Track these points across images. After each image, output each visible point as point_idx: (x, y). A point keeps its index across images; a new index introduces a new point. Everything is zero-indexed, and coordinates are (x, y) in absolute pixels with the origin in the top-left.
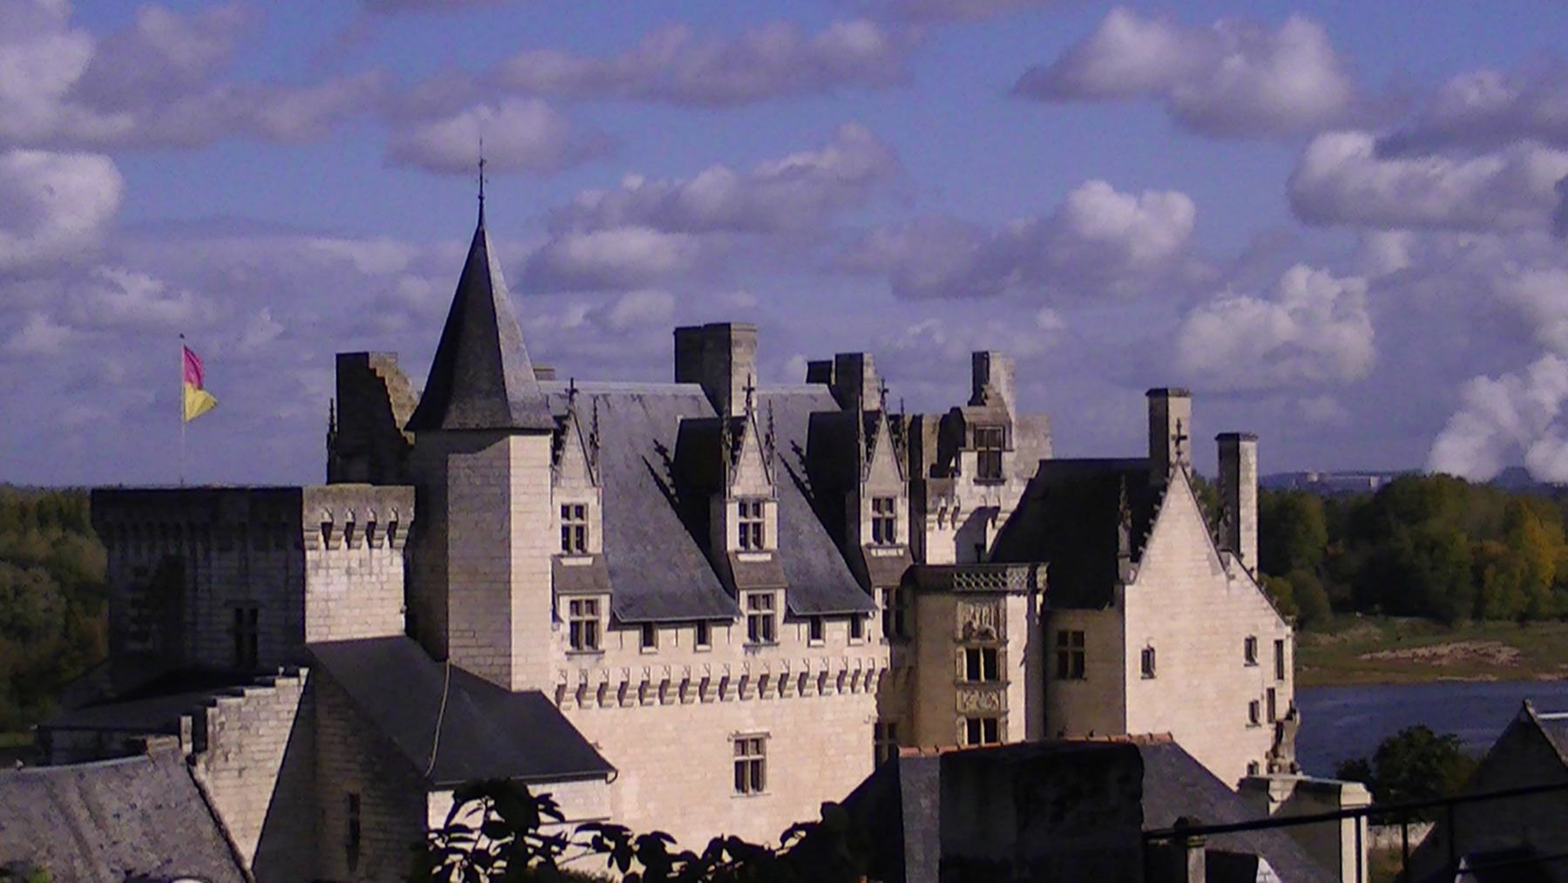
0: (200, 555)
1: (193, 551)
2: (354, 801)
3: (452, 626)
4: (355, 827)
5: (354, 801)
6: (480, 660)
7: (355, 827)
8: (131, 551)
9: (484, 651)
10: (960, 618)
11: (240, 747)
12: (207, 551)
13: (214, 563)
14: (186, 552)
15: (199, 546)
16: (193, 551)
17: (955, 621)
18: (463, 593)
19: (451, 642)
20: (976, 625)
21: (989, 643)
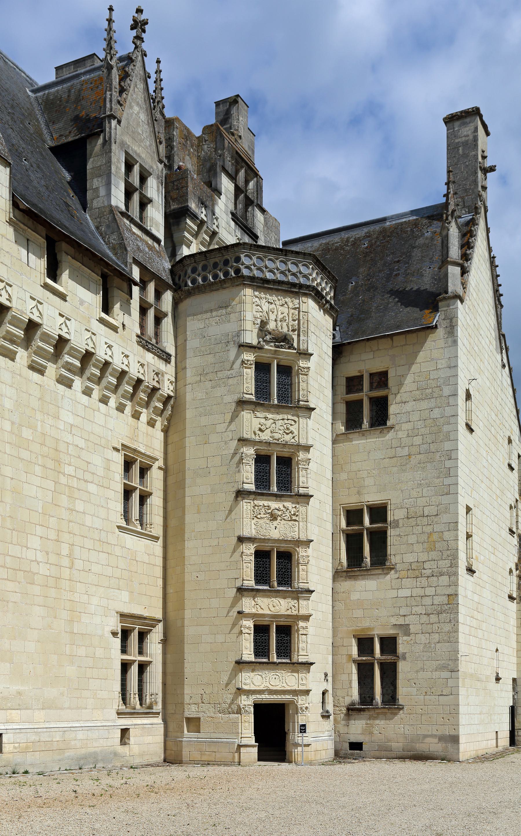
10: (249, 316)
17: (241, 320)
20: (271, 326)
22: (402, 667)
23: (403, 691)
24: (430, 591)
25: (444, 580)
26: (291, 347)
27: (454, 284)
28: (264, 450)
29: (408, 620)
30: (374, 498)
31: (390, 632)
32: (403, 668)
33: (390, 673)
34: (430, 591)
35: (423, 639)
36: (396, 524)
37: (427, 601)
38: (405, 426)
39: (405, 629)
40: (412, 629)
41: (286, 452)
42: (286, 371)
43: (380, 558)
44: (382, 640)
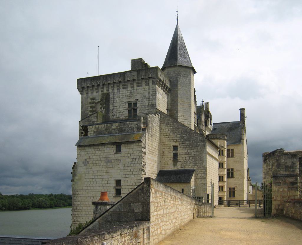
0: (116, 91)
1: (113, 90)
2: (175, 148)
3: (179, 114)
4: (175, 156)
5: (175, 148)
6: (185, 123)
7: (175, 156)
8: (90, 93)
9: (186, 121)
11: (151, 129)
12: (119, 89)
13: (121, 92)
14: (110, 91)
15: (116, 89)
16: (113, 90)
18: (181, 106)
19: (179, 118)
21: (223, 149)
22: (236, 192)
23: (236, 195)
24: (240, 181)
25: (242, 180)
26: (223, 148)
27: (243, 138)
28: (220, 162)
29: (237, 185)
30: (232, 167)
31: (234, 187)
32: (236, 192)
33: (234, 193)
34: (240, 181)
35: (239, 188)
36: (235, 171)
37: (239, 183)
38: (236, 157)
39: (236, 186)
40: (237, 186)
41: (222, 162)
42: (222, 151)
43: (232, 176)
44: (233, 188)
